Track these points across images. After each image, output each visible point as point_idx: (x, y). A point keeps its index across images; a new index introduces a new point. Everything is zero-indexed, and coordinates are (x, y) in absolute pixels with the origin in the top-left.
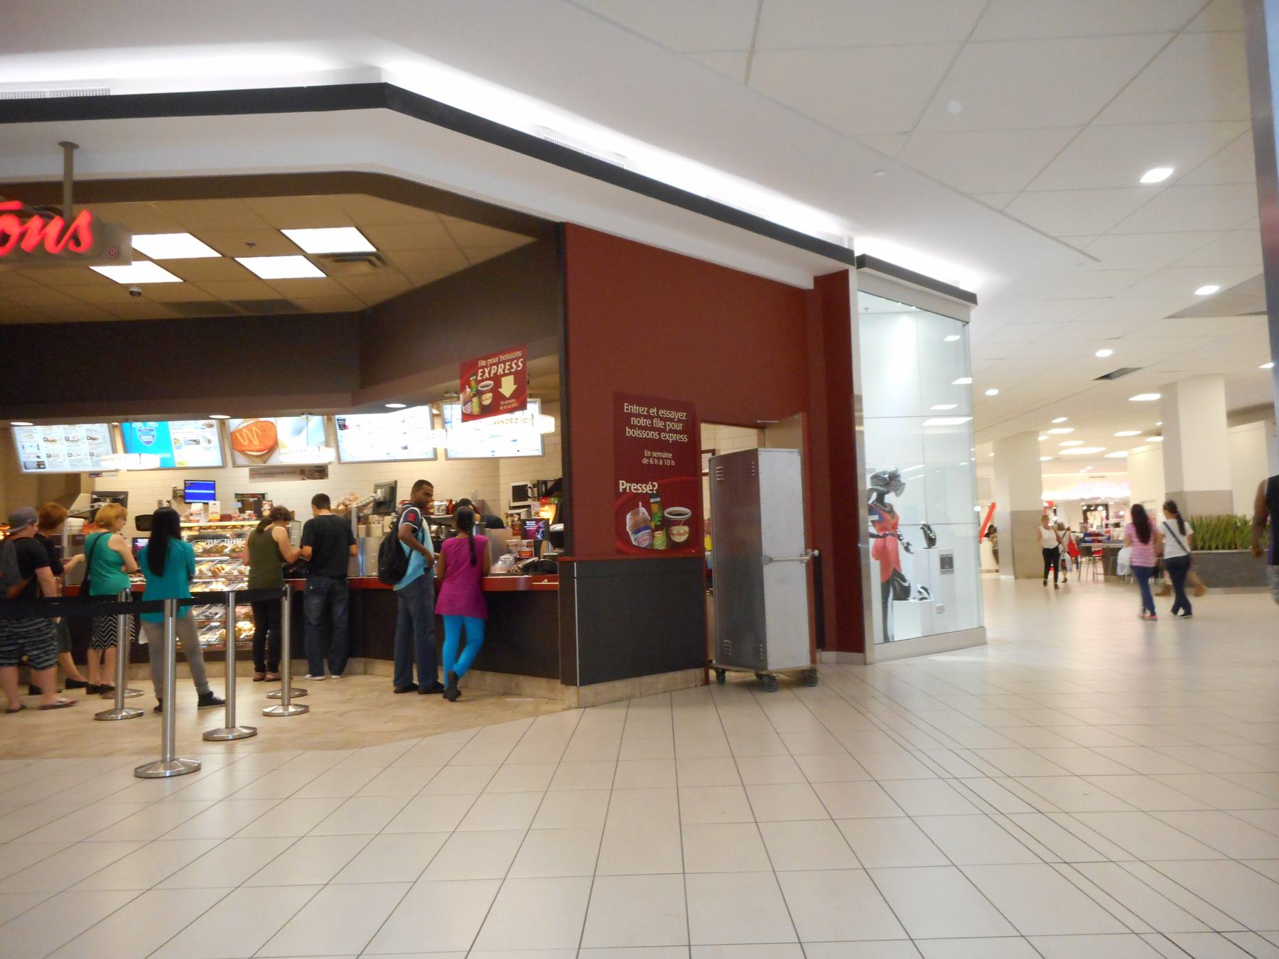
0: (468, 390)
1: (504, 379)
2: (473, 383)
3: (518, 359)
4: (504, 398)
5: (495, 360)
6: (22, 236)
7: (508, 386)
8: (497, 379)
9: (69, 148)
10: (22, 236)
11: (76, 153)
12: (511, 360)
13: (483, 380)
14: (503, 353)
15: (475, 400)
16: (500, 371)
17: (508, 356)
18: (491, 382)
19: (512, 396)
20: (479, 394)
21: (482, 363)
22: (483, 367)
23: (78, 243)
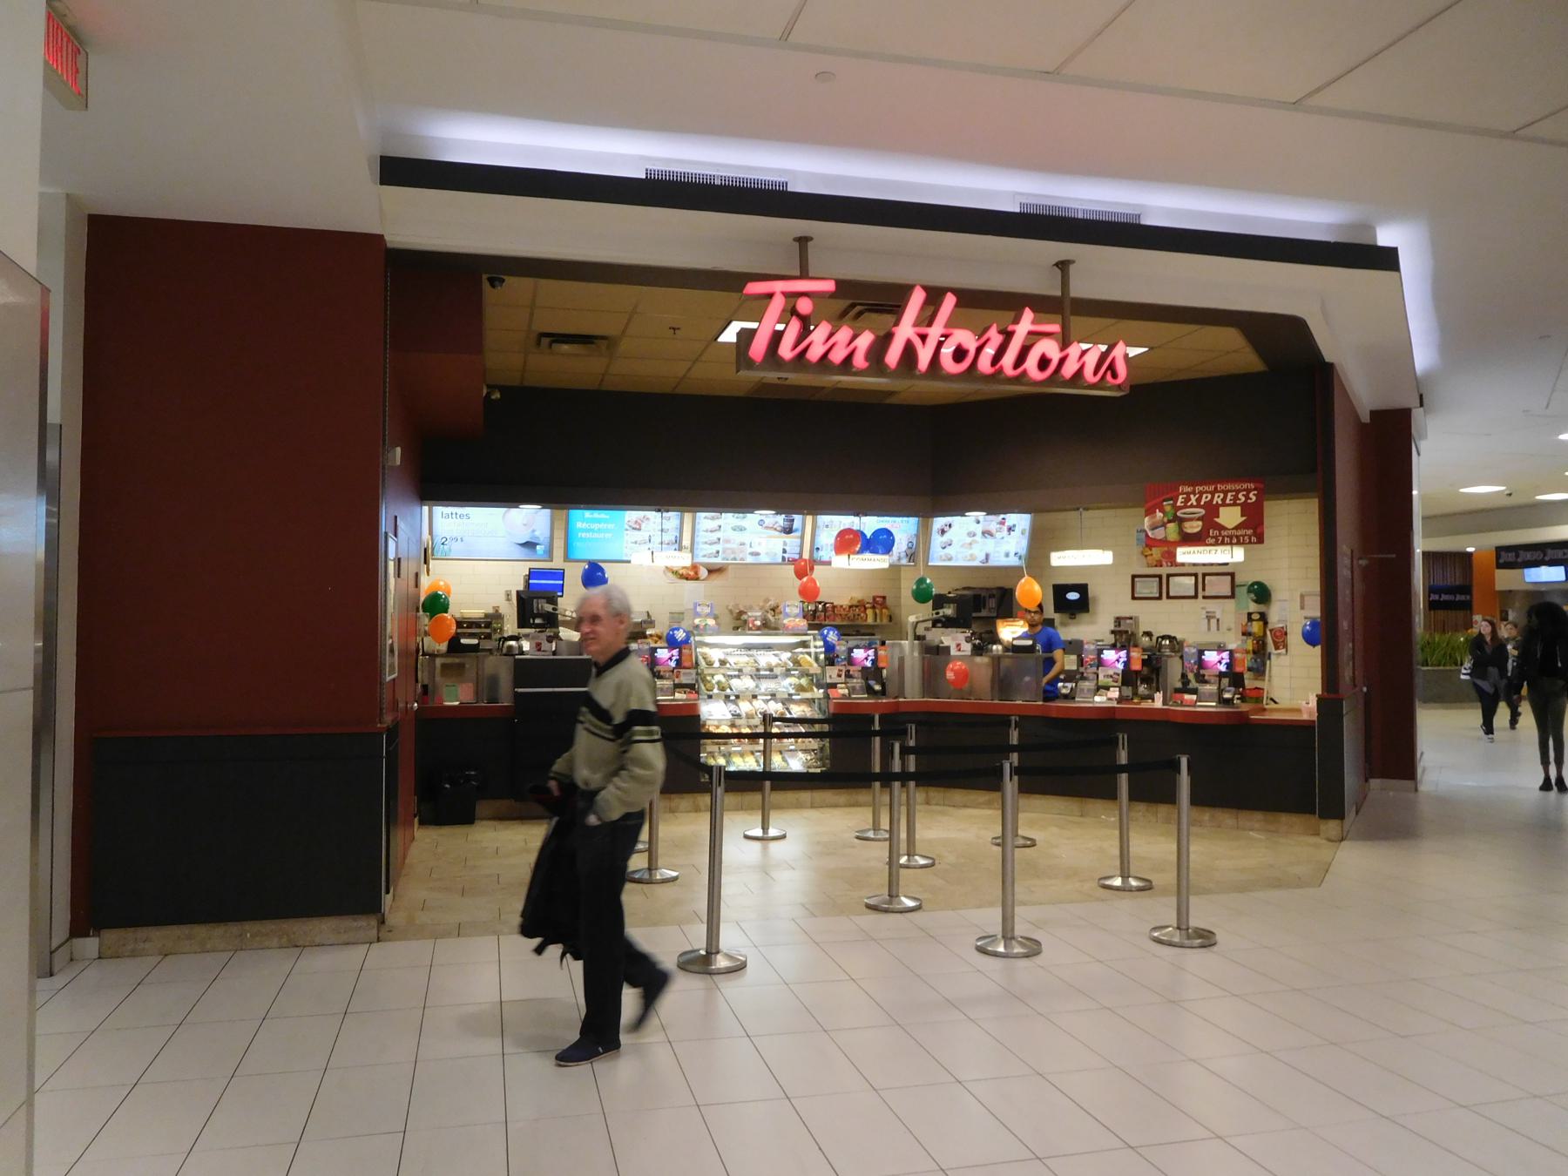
0: (1159, 515)
1: (1222, 509)
2: (1168, 508)
3: (1249, 491)
4: (1221, 528)
5: (1212, 488)
6: (1062, 361)
7: (1230, 517)
8: (1212, 510)
9: (1063, 266)
10: (1062, 361)
11: (1072, 268)
12: (1238, 492)
13: (1186, 507)
14: (1222, 482)
15: (1172, 527)
16: (1218, 499)
17: (1229, 487)
18: (1202, 511)
19: (1237, 528)
20: (1180, 521)
21: (1189, 489)
22: (1188, 494)
23: (1115, 376)
